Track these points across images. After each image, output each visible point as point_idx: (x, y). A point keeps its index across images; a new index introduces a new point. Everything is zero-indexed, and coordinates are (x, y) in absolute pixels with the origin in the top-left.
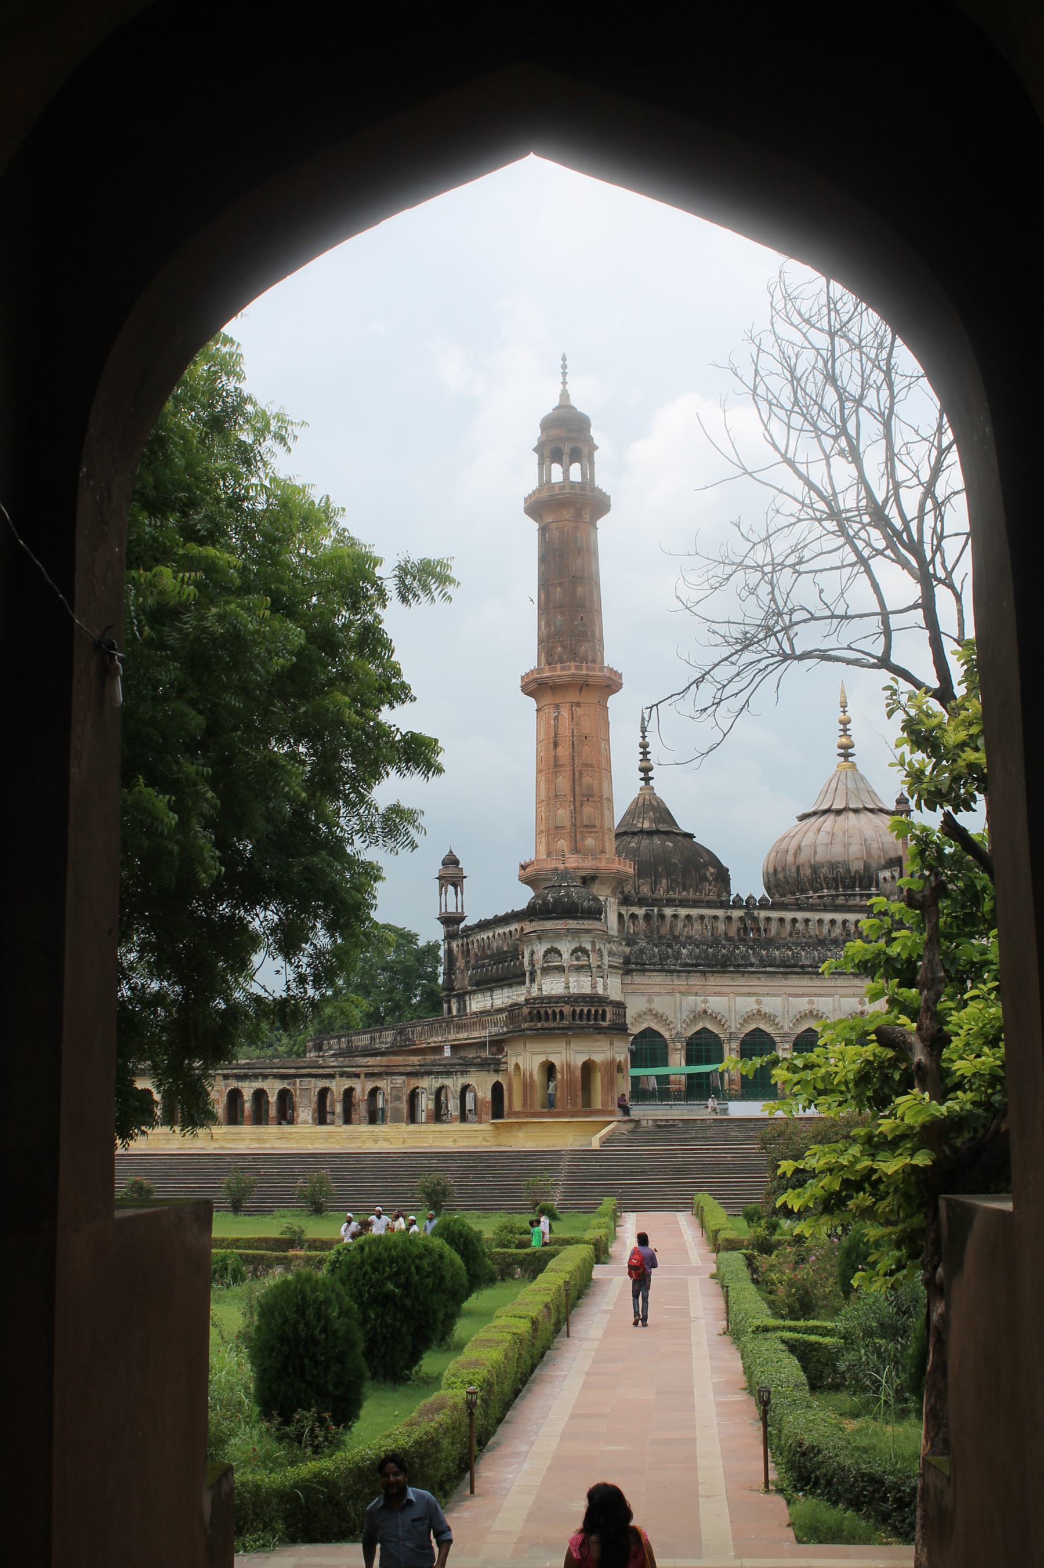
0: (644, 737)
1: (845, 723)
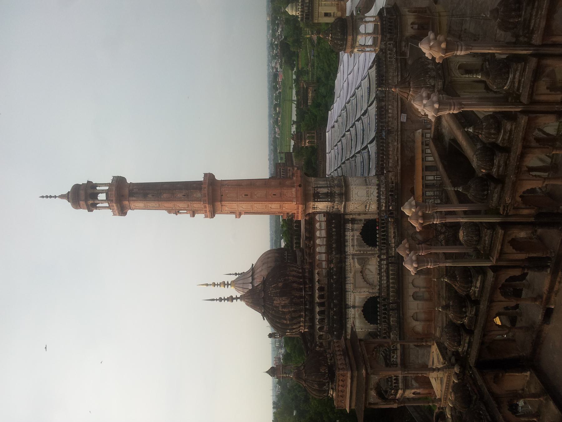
0: (217, 300)
1: (214, 284)
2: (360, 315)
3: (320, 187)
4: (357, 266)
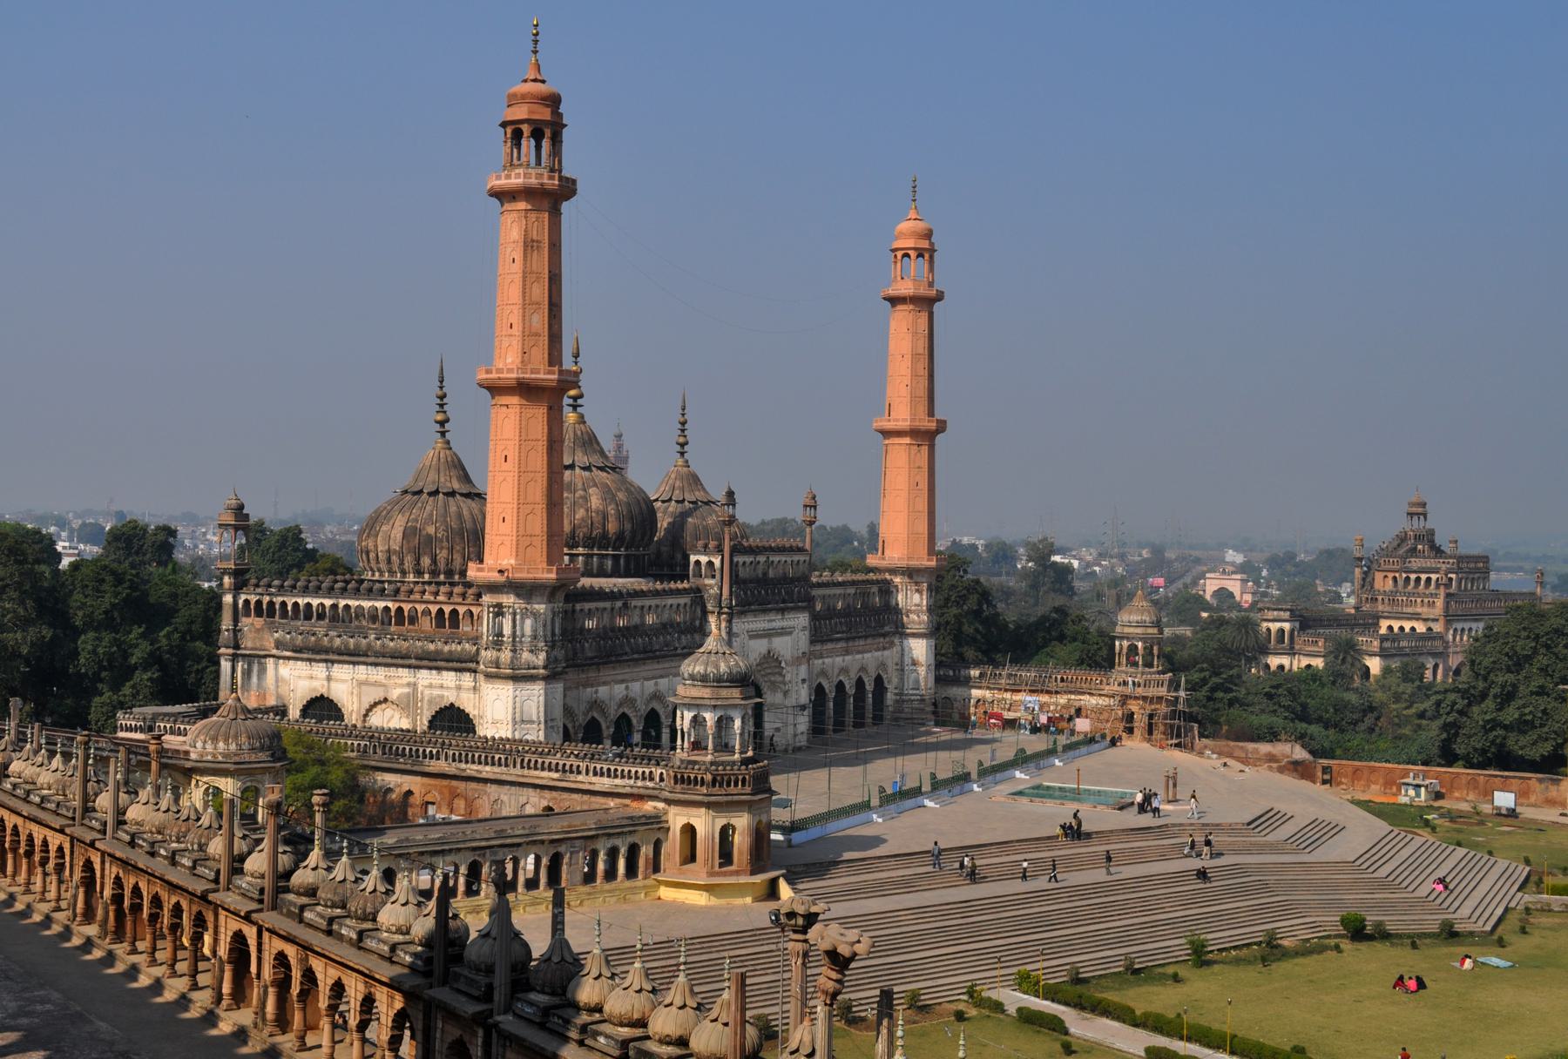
2: (315, 690)
3: (514, 621)
4: (395, 694)
